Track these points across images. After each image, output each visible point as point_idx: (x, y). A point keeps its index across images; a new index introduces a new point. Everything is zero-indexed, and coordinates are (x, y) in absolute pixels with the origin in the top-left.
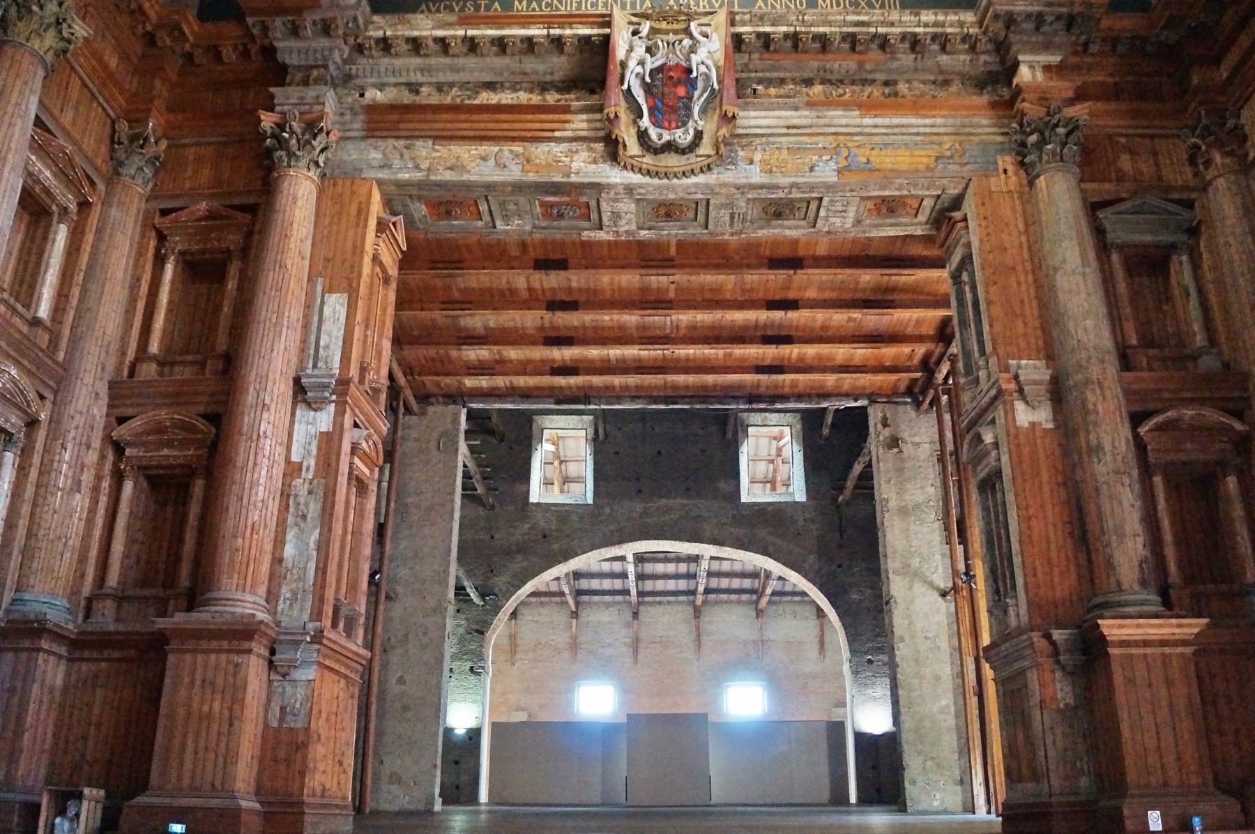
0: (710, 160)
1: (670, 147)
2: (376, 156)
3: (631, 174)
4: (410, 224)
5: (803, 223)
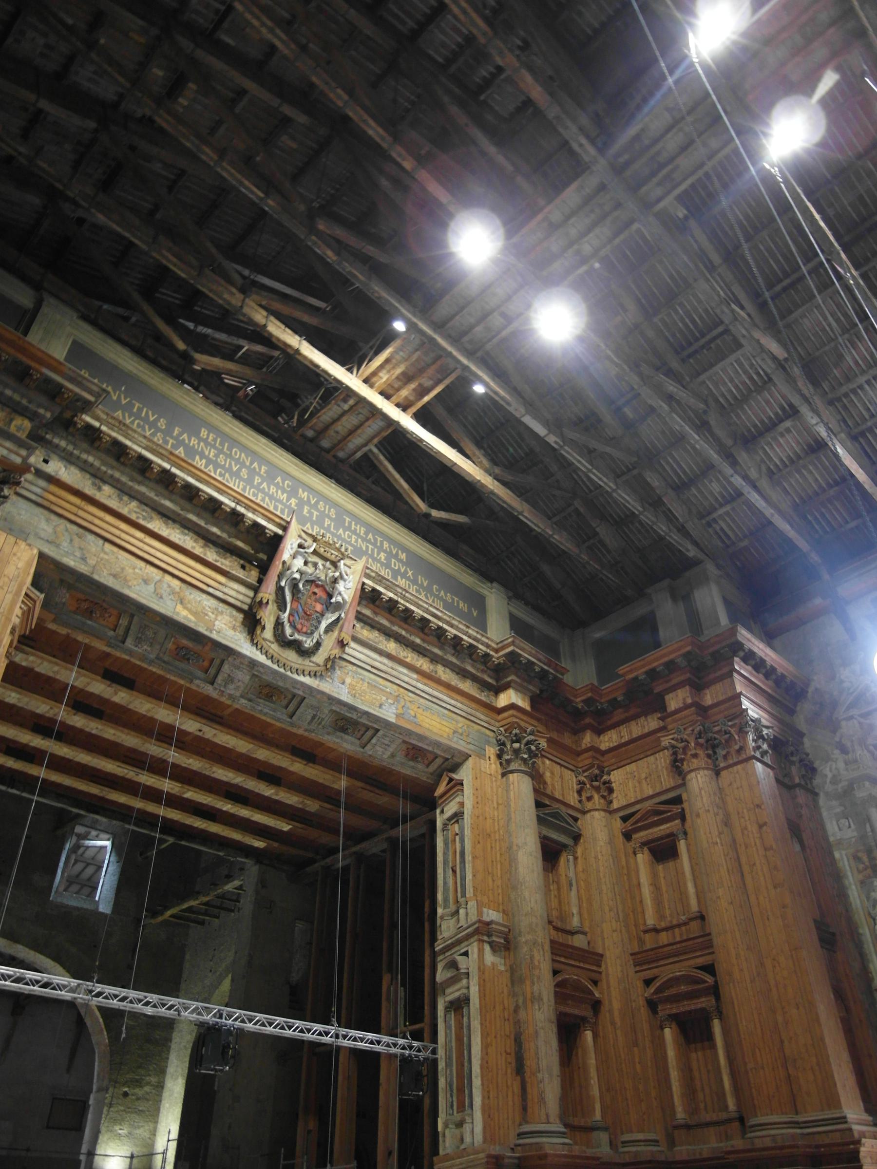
0: (317, 669)
1: (295, 646)
3: (258, 653)
5: (358, 742)
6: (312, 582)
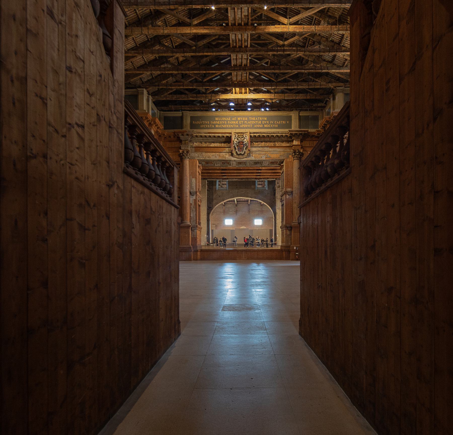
1: (241, 154)
2: (197, 155)
4: (202, 165)
6: (239, 142)
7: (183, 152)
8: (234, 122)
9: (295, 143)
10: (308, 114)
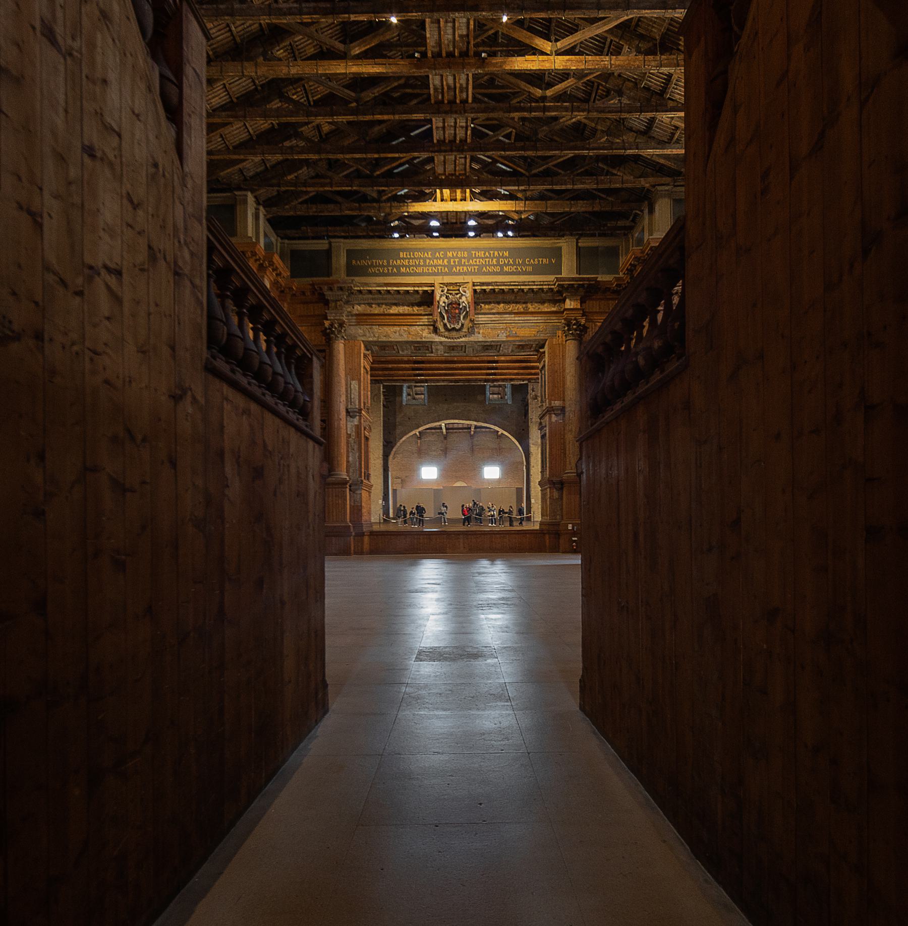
1: (454, 329)
2: (360, 331)
4: (372, 352)
6: (451, 304)
7: (332, 325)
8: (440, 262)
9: (569, 304)
10: (597, 244)
